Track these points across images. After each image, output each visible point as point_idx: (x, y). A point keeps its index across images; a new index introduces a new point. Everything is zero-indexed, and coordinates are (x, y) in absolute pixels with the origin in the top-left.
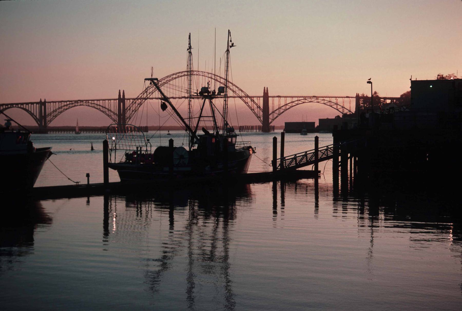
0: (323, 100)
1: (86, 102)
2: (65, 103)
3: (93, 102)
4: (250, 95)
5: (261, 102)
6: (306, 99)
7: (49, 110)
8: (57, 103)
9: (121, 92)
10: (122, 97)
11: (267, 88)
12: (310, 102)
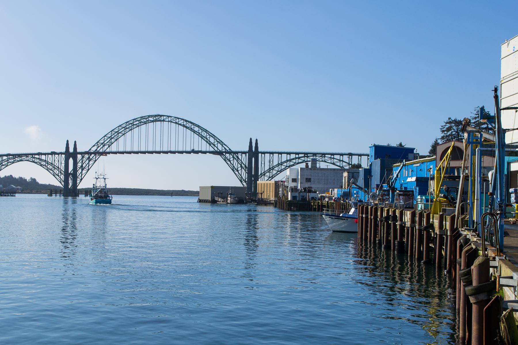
4: (233, 149)
5: (245, 159)
6: (308, 157)
10: (254, 149)
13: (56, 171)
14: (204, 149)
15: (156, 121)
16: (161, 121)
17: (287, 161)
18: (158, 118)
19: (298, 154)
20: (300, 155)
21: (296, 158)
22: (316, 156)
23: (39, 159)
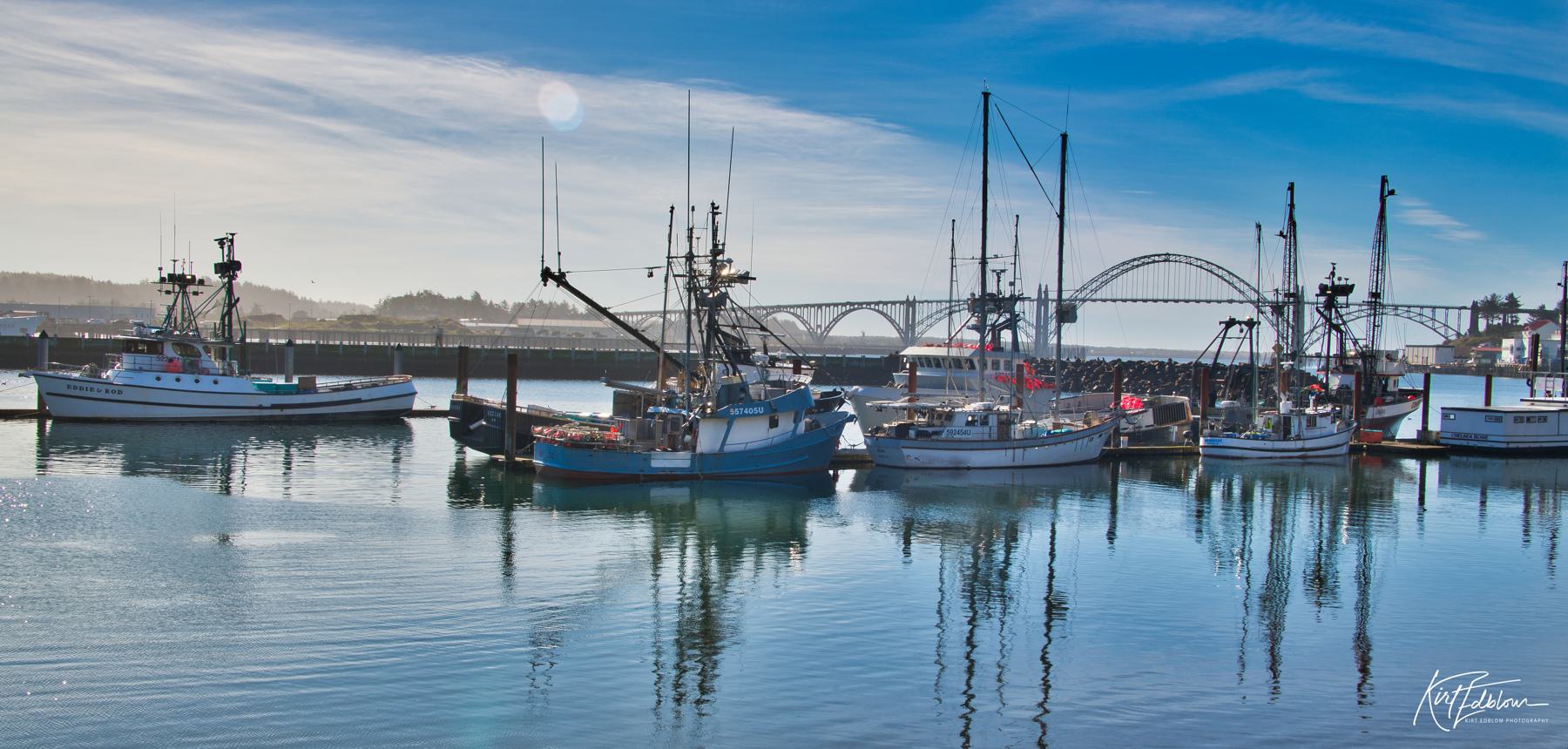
0: (1407, 311)
8: (934, 304)
15: (1165, 261)
16: (1169, 261)
18: (1167, 258)
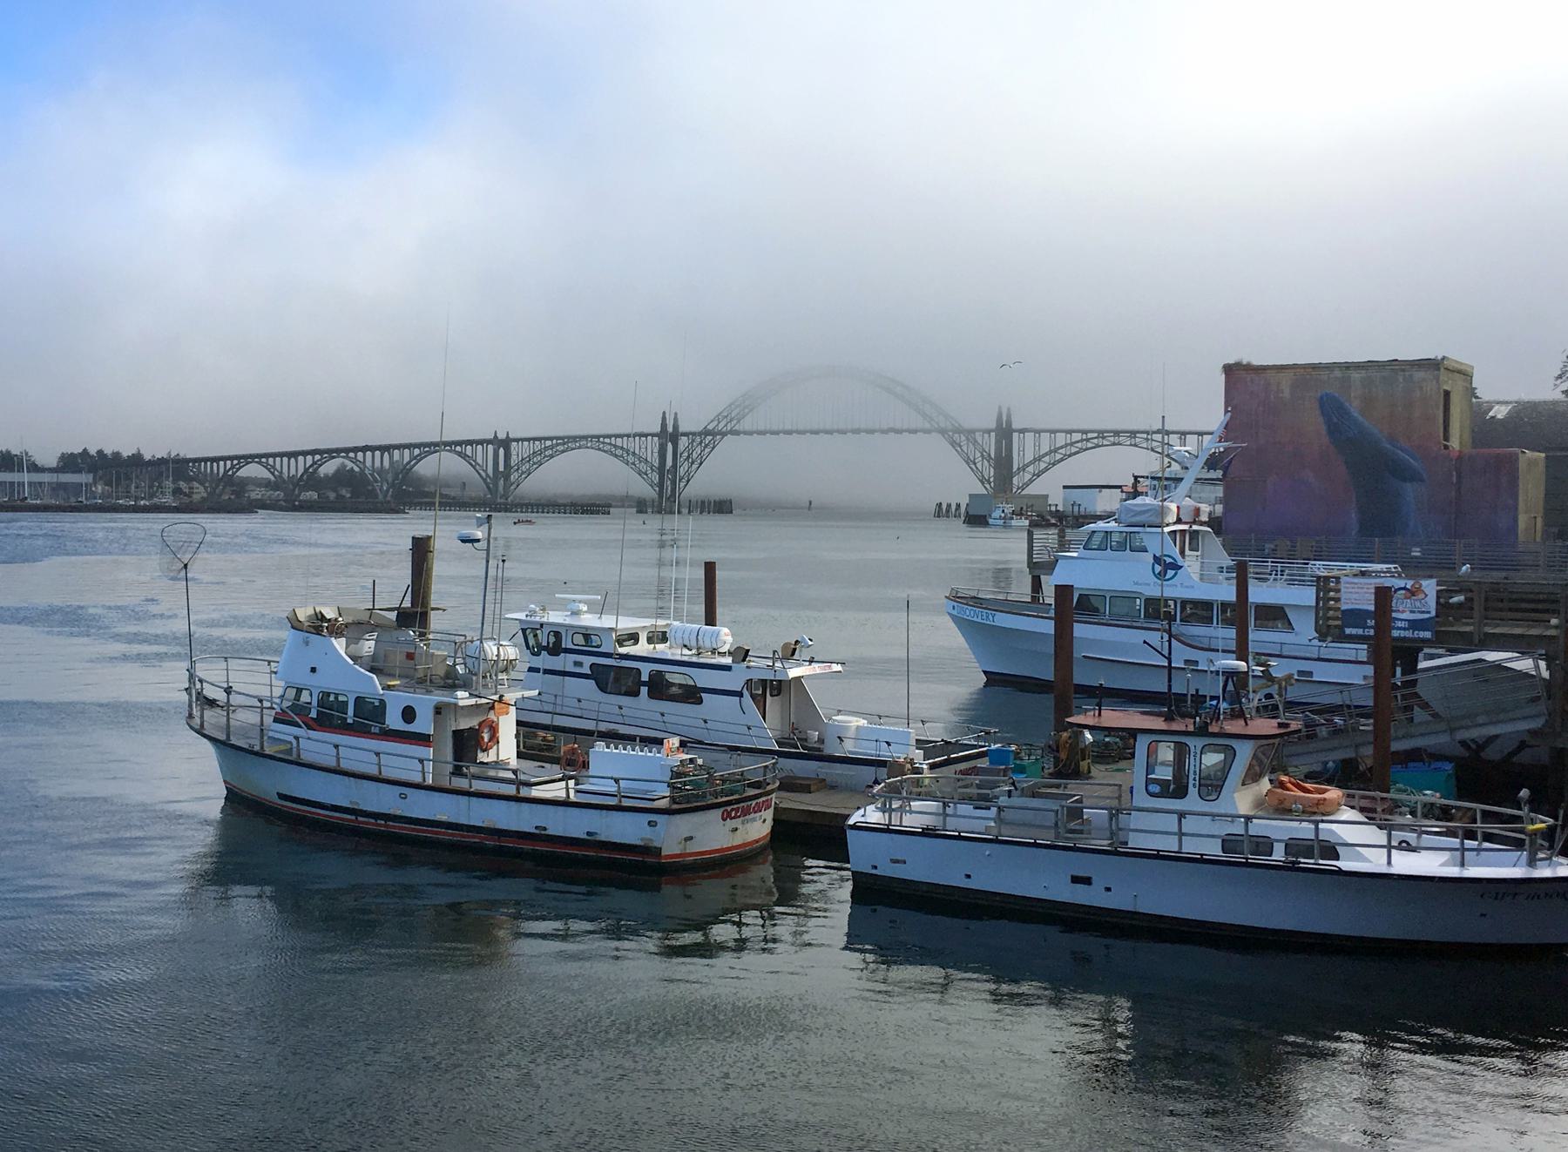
1: (591, 441)
2: (548, 443)
3: (607, 440)
4: (967, 425)
5: (990, 442)
6: (1104, 438)
7: (514, 457)
8: (649, 438)
9: (667, 416)
11: (1009, 409)
12: (1114, 444)
13: (643, 467)
14: (913, 426)
17: (1066, 445)
19: (1085, 432)
20: (1090, 435)
21: (1082, 440)
22: (1119, 437)
23: (610, 444)
